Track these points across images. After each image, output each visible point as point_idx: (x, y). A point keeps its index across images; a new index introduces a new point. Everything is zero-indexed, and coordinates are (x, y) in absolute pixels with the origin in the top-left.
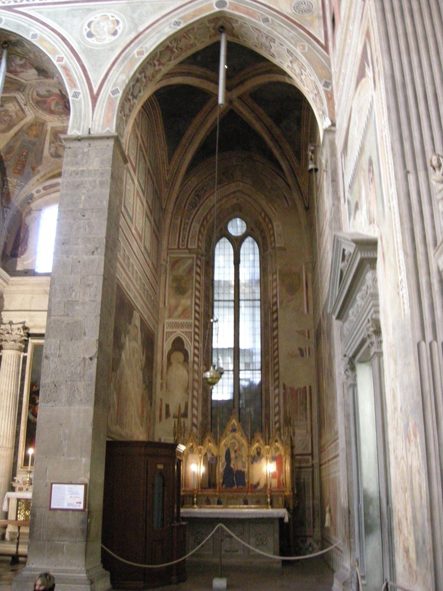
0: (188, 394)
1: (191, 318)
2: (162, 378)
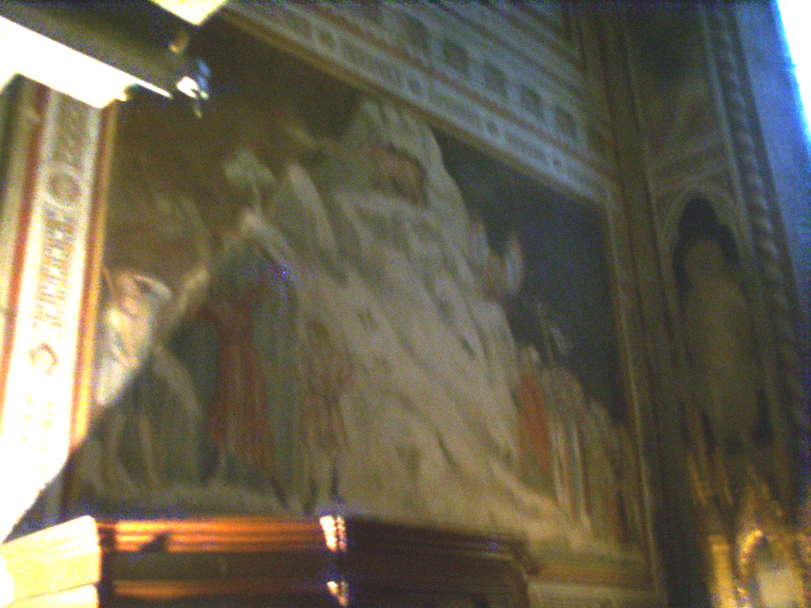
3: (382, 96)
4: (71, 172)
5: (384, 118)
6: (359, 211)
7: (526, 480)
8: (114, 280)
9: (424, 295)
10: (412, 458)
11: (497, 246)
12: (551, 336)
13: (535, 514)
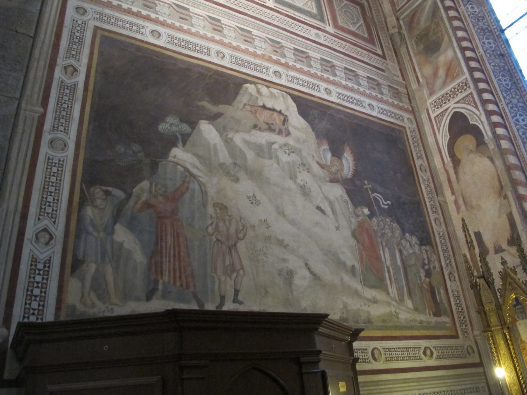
0: (506, 197)
1: (463, 74)
2: (453, 193)
3: (256, 81)
5: (258, 91)
6: (246, 142)
7: (365, 283)
8: (88, 191)
9: (289, 184)
11: (337, 153)
12: (375, 198)
13: (375, 301)
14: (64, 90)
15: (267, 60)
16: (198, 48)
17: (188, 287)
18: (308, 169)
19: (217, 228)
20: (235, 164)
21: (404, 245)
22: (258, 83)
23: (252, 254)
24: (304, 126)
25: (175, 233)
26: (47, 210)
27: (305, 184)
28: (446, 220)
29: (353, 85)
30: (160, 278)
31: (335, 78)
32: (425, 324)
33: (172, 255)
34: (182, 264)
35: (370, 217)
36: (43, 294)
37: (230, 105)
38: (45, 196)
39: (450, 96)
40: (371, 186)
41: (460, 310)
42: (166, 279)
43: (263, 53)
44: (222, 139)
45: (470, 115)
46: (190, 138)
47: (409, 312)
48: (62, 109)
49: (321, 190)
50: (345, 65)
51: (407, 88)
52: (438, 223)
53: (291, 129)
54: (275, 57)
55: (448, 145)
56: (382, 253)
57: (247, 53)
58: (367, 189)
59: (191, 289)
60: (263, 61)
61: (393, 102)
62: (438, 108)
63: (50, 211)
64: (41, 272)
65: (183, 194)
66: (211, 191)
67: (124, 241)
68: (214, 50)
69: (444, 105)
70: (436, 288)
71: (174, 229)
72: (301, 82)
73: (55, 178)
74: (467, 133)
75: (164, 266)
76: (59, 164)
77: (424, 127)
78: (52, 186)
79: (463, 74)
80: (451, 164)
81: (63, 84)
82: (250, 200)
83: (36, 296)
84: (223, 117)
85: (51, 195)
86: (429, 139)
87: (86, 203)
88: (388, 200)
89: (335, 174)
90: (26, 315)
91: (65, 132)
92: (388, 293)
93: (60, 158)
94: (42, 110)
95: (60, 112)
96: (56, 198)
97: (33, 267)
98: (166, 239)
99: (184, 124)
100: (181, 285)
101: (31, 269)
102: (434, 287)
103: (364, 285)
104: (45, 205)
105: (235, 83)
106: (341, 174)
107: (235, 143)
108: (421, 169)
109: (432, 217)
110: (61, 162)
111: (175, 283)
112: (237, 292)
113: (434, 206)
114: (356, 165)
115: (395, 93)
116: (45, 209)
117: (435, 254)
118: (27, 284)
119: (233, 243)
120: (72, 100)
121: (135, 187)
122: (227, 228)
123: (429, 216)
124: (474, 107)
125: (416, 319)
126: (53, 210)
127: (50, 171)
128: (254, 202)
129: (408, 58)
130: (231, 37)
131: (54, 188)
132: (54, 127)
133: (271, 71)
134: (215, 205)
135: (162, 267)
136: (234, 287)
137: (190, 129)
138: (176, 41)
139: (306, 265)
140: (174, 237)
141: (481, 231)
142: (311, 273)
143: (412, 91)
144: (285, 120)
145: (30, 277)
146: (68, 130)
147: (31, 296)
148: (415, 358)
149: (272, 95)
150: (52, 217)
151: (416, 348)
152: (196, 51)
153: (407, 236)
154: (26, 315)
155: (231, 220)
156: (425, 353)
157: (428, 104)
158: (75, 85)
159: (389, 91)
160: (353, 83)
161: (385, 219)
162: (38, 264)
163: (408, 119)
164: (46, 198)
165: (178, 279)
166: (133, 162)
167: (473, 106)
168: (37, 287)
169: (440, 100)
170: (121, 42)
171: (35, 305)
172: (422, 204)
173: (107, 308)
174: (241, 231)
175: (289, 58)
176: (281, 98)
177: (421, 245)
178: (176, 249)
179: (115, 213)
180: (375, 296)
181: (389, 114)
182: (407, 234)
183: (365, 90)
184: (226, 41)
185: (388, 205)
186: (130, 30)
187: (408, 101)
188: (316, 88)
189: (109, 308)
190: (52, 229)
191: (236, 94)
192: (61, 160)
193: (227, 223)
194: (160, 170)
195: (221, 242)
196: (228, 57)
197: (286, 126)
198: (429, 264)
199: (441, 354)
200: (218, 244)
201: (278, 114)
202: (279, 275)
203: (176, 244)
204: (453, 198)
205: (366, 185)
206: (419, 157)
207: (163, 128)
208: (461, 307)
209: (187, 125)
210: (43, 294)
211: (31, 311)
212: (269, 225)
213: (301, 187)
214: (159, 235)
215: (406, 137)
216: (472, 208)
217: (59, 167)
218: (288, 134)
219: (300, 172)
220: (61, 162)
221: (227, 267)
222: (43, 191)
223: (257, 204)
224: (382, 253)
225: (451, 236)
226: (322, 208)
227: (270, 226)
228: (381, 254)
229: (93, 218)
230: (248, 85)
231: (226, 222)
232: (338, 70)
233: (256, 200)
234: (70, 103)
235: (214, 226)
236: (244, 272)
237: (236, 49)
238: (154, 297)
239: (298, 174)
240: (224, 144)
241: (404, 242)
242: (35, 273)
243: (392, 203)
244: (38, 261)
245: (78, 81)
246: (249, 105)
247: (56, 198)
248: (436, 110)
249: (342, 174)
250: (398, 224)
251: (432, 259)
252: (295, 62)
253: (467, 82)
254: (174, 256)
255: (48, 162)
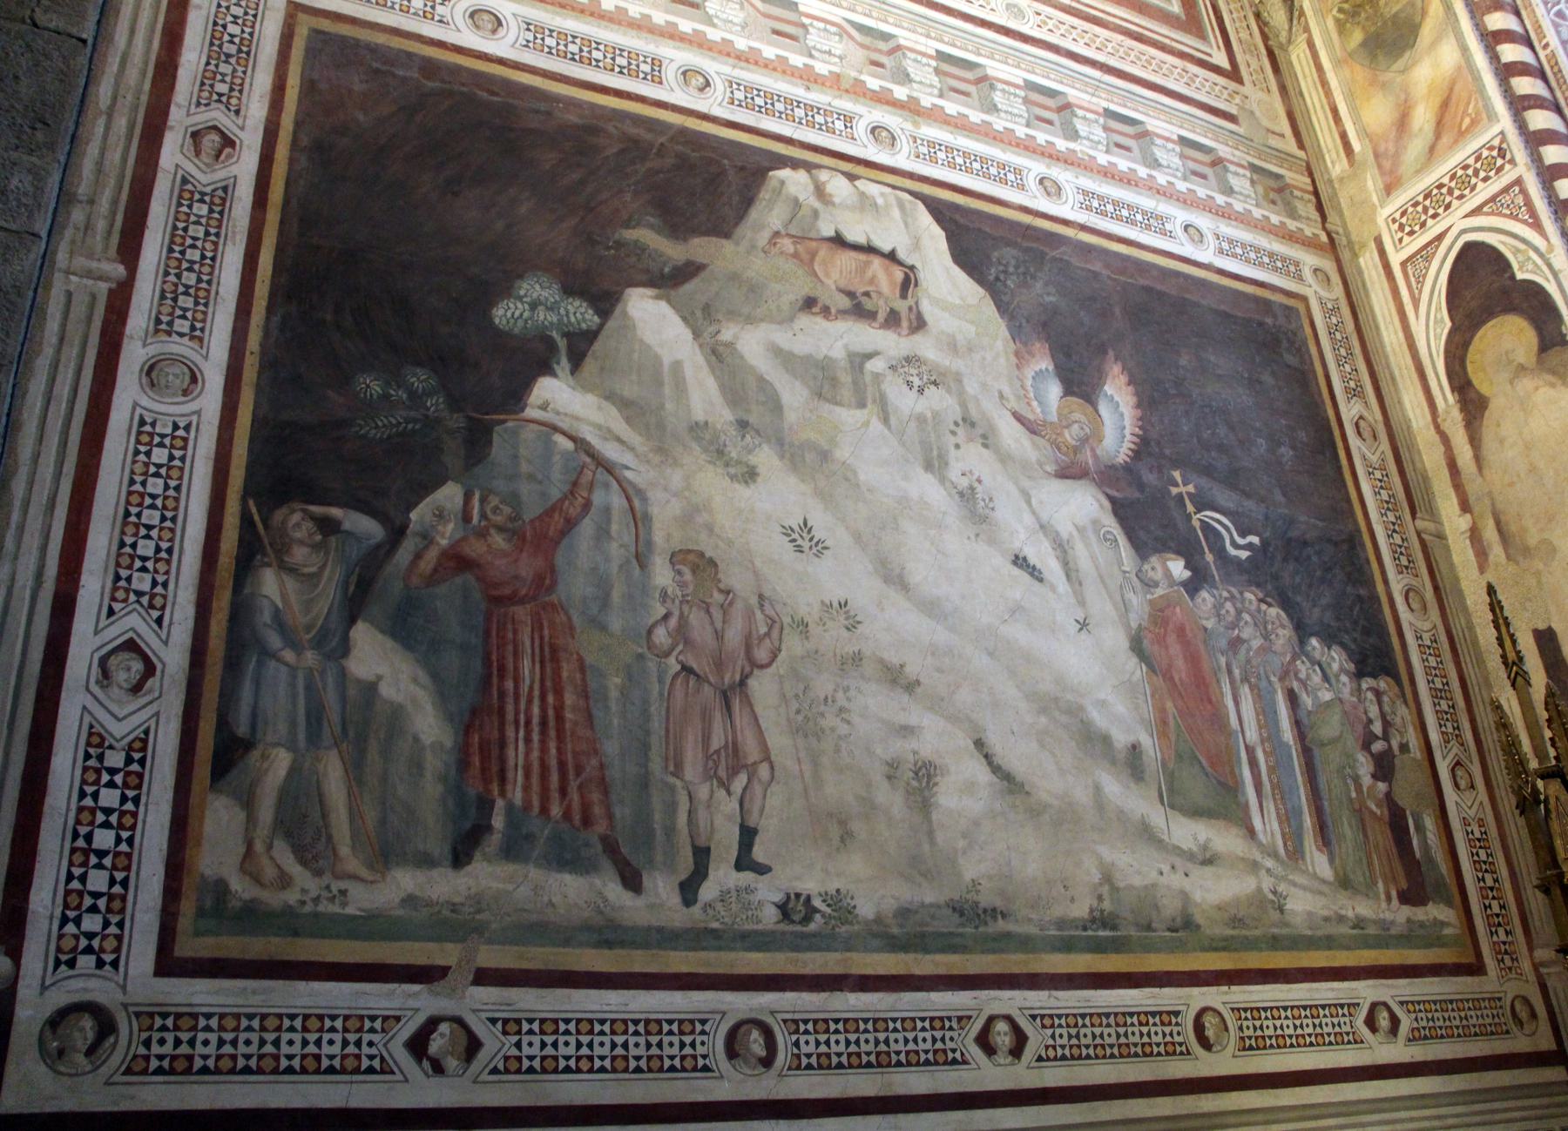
1: (1492, 117)
2: (1465, 507)
3: (812, 158)
4: (180, 347)
5: (820, 191)
6: (777, 352)
7: (1175, 800)
10: (925, 775)
12: (1206, 527)
14: (190, 207)
15: (847, 91)
16: (622, 61)
17: (587, 821)
18: (984, 437)
19: (682, 634)
20: (743, 425)
21: (1303, 675)
22: (819, 167)
23: (798, 712)
24: (972, 301)
25: (547, 649)
26: (135, 585)
27: (976, 485)
28: (1443, 592)
29: (1133, 166)
30: (496, 793)
31: (1072, 145)
32: (1372, 930)
33: (536, 720)
34: (569, 746)
35: (1192, 586)
36: (124, 847)
37: (727, 235)
38: (129, 540)
39: (1450, 192)
40: (1196, 487)
41: (1490, 882)
42: (518, 797)
43: (836, 69)
44: (701, 346)
45: (1516, 251)
46: (597, 346)
47: (1321, 893)
48: (185, 265)
49: (1029, 502)
50: (1105, 104)
51: (1311, 175)
52: (1415, 606)
53: (926, 308)
54: (873, 84)
55: (1447, 351)
56: (1230, 703)
57: (784, 72)
58: (1180, 497)
59: (601, 827)
60: (835, 97)
61: (1267, 218)
62: (1411, 233)
63: (146, 587)
64: (118, 779)
65: (570, 524)
66: (664, 513)
67: (380, 678)
68: (674, 66)
69: (1430, 222)
70: (1408, 812)
71: (542, 638)
72: (959, 160)
73: (160, 482)
74: (1510, 309)
75: (511, 752)
76: (174, 438)
77: (1367, 295)
78: (153, 507)
79: (1492, 117)
80: (1456, 414)
81: (189, 187)
82: (794, 540)
83: (101, 854)
84: (703, 275)
85: (148, 537)
86: (1384, 333)
87: (259, 557)
88: (1250, 533)
89: (1076, 450)
90: (71, 914)
91: (192, 338)
92: (1251, 832)
93: (177, 419)
94: (120, 270)
95: (179, 276)
96: (164, 545)
97: (92, 763)
98: (516, 669)
99: (577, 303)
100: (567, 815)
101: (85, 769)
102: (1404, 811)
103: (1172, 807)
104: (130, 567)
105: (742, 169)
106: (1093, 450)
107: (742, 357)
108: (1359, 433)
109: (1397, 584)
110: (181, 433)
111: (544, 810)
112: (748, 835)
113: (1403, 550)
114: (1144, 422)
115: (1273, 189)
116: (129, 579)
117: (1406, 702)
118: (72, 814)
119: (738, 677)
120: (217, 235)
121: (416, 504)
122: (716, 632)
123: (1386, 581)
124: (1529, 225)
125: (1343, 912)
126: (154, 583)
127: (146, 460)
128: (806, 545)
129: (1315, 76)
130: (731, 22)
131: (157, 514)
132: (158, 321)
133: (861, 128)
134: (676, 558)
135: (502, 760)
136: (739, 820)
137: (596, 319)
138: (550, 42)
139: (979, 744)
140: (542, 662)
141: (1554, 626)
142: (996, 769)
143: (1330, 181)
144: (909, 282)
145: (82, 795)
146: (202, 330)
147: (86, 852)
148: (1341, 1040)
149: (865, 203)
150: (152, 606)
151: (1342, 1006)
152: (617, 69)
153: (1314, 648)
154: (71, 914)
155: (731, 604)
156: (1371, 1023)
157: (1381, 221)
158: (225, 189)
159: (1253, 182)
160: (1134, 160)
161: (1241, 593)
162: (108, 752)
163: (1316, 270)
164: (134, 546)
165: (555, 795)
166: (410, 426)
167: (1524, 222)
168: (106, 825)
169: (1420, 208)
170: (373, 49)
171: (98, 881)
172: (1363, 545)
173: (328, 887)
174: (761, 639)
175: (921, 83)
176: (896, 213)
177: (1359, 674)
178: (550, 699)
179: (352, 588)
180: (1208, 840)
181: (1253, 255)
182: (1314, 642)
183: (1172, 180)
184: (714, 35)
185: (1249, 546)
186: (401, 10)
187: (1315, 215)
188: (1011, 177)
189: (334, 890)
190: (150, 639)
191: (748, 201)
192: (182, 425)
193: (717, 614)
194: (499, 449)
195: (697, 675)
196: (719, 85)
197: (910, 301)
198: (1386, 737)
199: (1424, 1023)
200: (688, 682)
201: (887, 262)
202: (889, 778)
203: (549, 684)
204: (1464, 522)
205: (1177, 485)
206: (1355, 393)
207: (509, 314)
208: (1494, 872)
209: (585, 304)
210: (124, 847)
211: (88, 901)
212: (858, 619)
213: (961, 494)
214: (494, 658)
215: (1308, 330)
216: (1527, 551)
217: (172, 446)
218: (919, 324)
219: (957, 446)
220: (181, 433)
221: (715, 757)
222: (125, 523)
223: (814, 550)
224: (1230, 703)
225: (1455, 643)
226: (1032, 560)
227: (859, 622)
228: (1226, 707)
229: (280, 605)
230: (785, 173)
231: (711, 610)
232: (1084, 118)
233: (811, 540)
234: (208, 246)
235: (673, 622)
236: (772, 768)
237: (747, 61)
238: (478, 855)
239: (952, 451)
240: (708, 362)
241: (1302, 667)
242: (97, 782)
243: (1265, 544)
244: (107, 744)
245: (235, 177)
246: (788, 235)
247: (164, 545)
248: (1406, 239)
249: (1098, 452)
250: (1284, 609)
251: (1398, 720)
252: (941, 96)
253: (1504, 146)
254: (544, 723)
255: (139, 433)
